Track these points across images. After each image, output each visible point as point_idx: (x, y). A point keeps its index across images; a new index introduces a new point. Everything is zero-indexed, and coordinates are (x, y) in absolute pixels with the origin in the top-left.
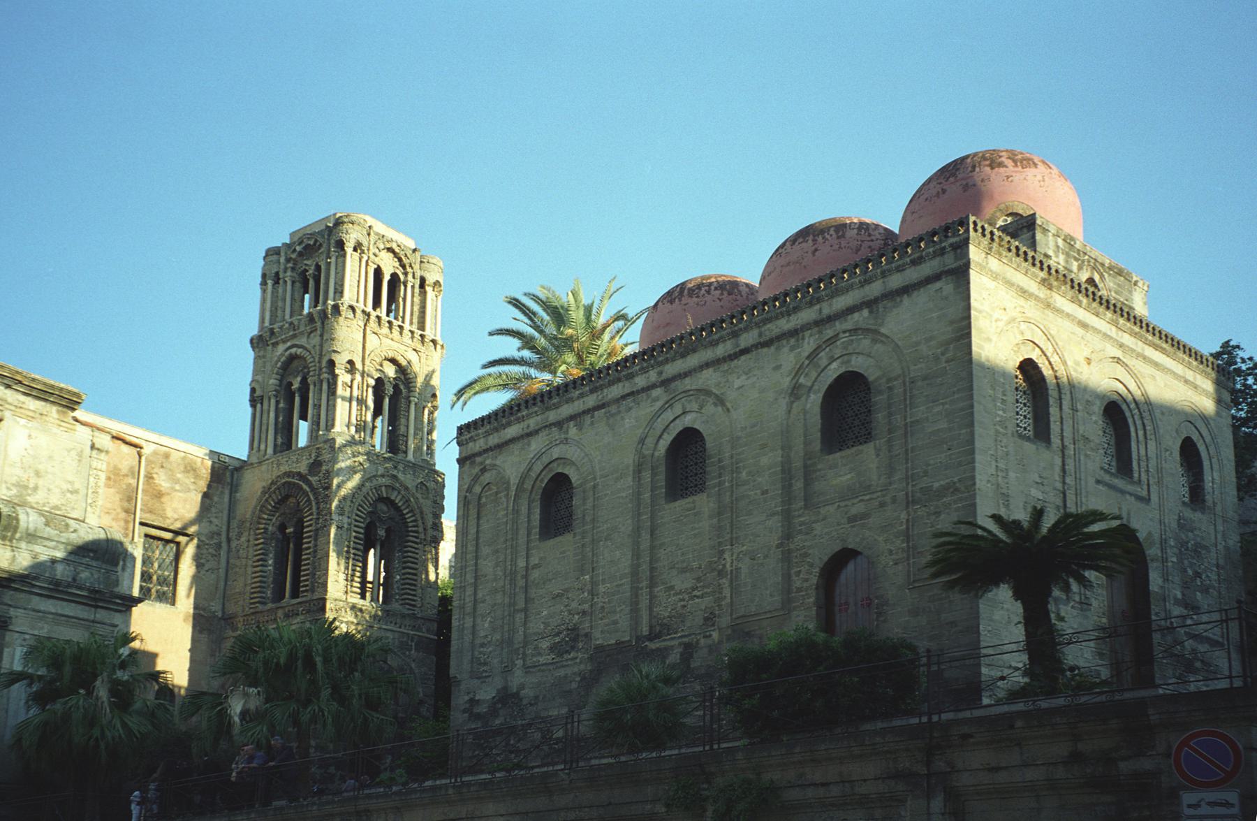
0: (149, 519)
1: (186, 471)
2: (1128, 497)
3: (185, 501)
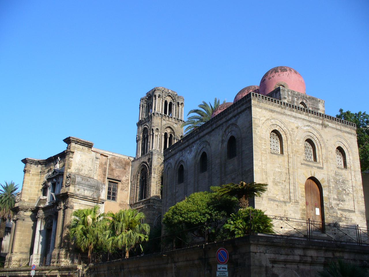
0: (110, 177)
1: (119, 163)
2: (314, 168)
3: (119, 171)
